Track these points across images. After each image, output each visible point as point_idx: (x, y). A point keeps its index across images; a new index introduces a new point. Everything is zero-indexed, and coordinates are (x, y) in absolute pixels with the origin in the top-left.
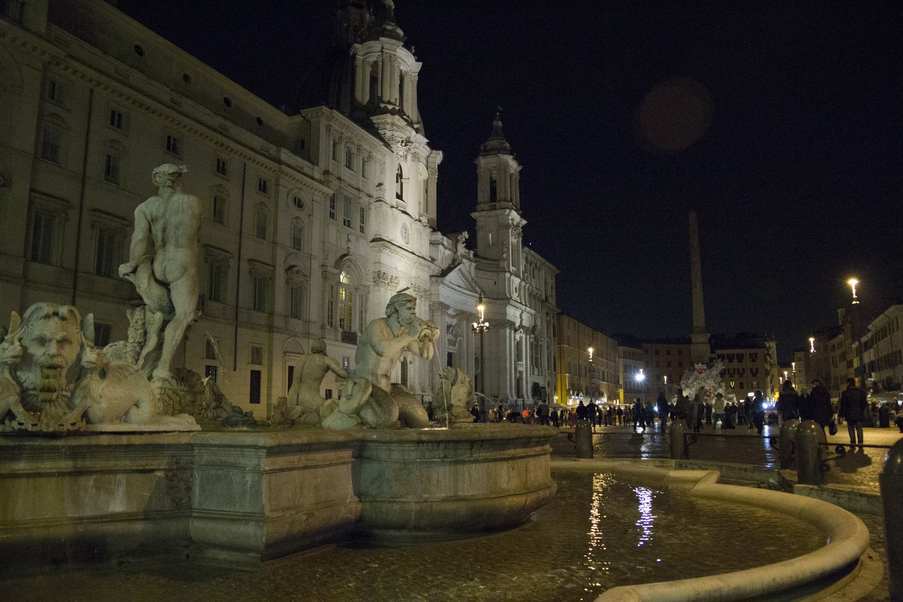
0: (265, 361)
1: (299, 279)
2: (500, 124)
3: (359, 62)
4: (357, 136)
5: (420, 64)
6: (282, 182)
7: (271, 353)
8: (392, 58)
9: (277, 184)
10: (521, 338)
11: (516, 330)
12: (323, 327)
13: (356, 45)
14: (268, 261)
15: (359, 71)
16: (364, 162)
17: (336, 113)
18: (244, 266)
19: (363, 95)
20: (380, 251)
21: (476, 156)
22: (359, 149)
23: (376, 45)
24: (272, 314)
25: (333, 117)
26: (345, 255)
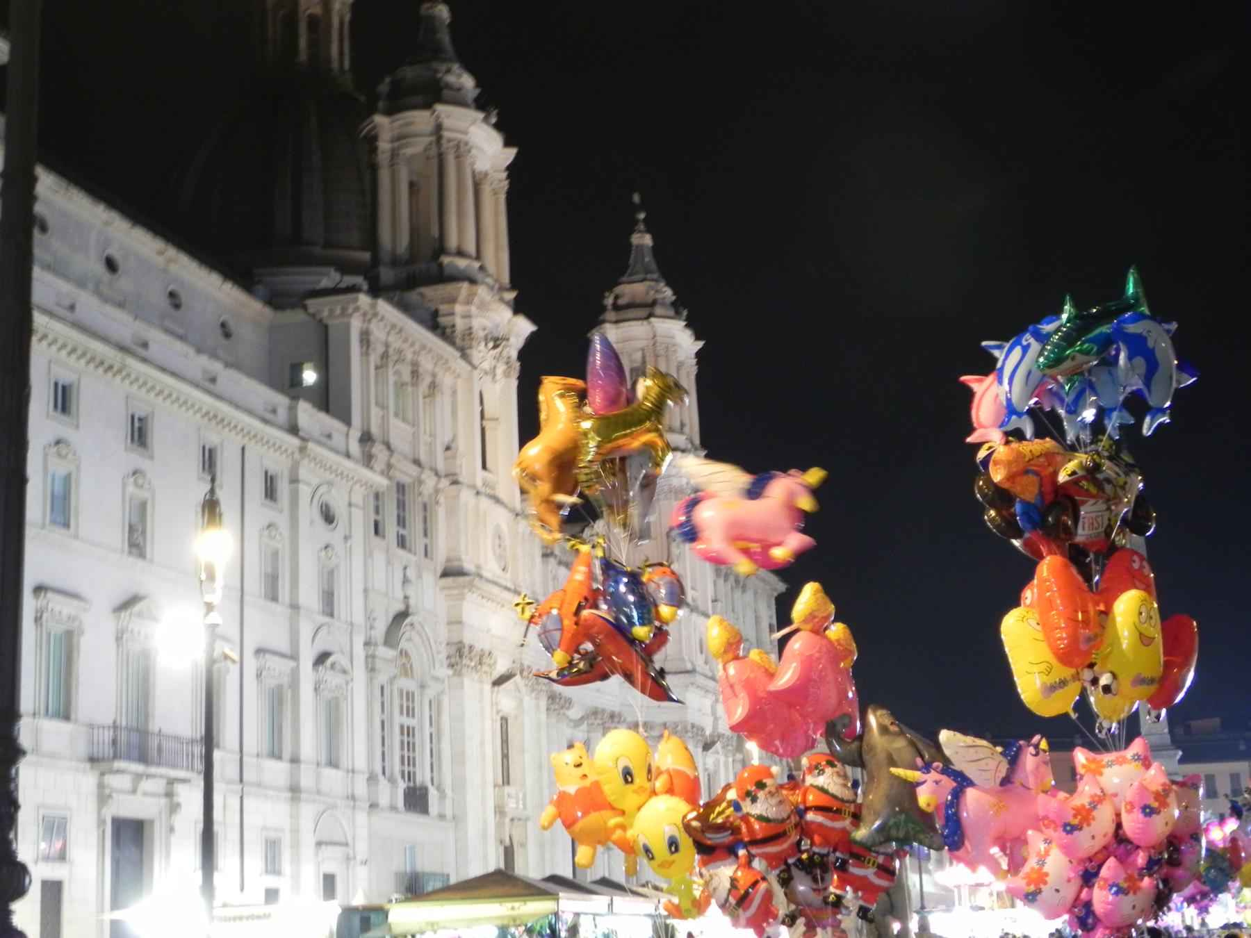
0: (286, 867)
1: (332, 679)
2: (647, 240)
3: (383, 157)
4: (413, 344)
5: (512, 153)
6: (303, 473)
7: (296, 845)
8: (462, 149)
9: (294, 480)
10: (717, 763)
11: (707, 747)
12: (372, 779)
13: (379, 119)
14: (284, 646)
15: (384, 176)
16: (400, 386)
17: (383, 306)
18: (251, 665)
19: (394, 233)
20: (461, 597)
21: (594, 318)
22: (415, 373)
23: (420, 120)
24: (295, 760)
25: (375, 315)
26: (402, 616)
